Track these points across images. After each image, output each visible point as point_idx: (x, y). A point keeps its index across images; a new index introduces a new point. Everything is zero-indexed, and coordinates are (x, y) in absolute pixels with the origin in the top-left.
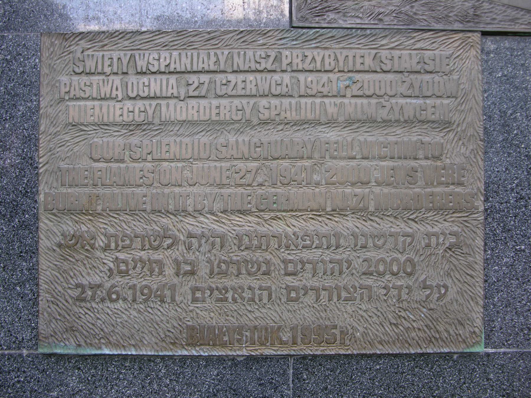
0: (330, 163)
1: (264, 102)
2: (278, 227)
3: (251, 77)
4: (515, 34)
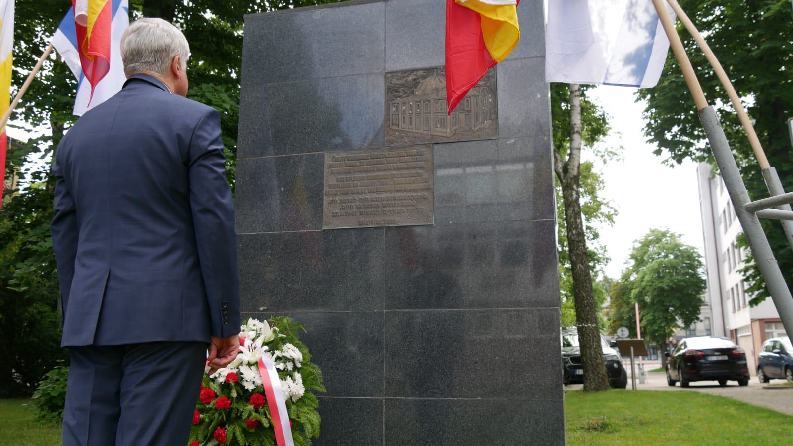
0: (394, 179)
1: (378, 165)
2: (381, 196)
3: (375, 160)
4: (456, 142)
